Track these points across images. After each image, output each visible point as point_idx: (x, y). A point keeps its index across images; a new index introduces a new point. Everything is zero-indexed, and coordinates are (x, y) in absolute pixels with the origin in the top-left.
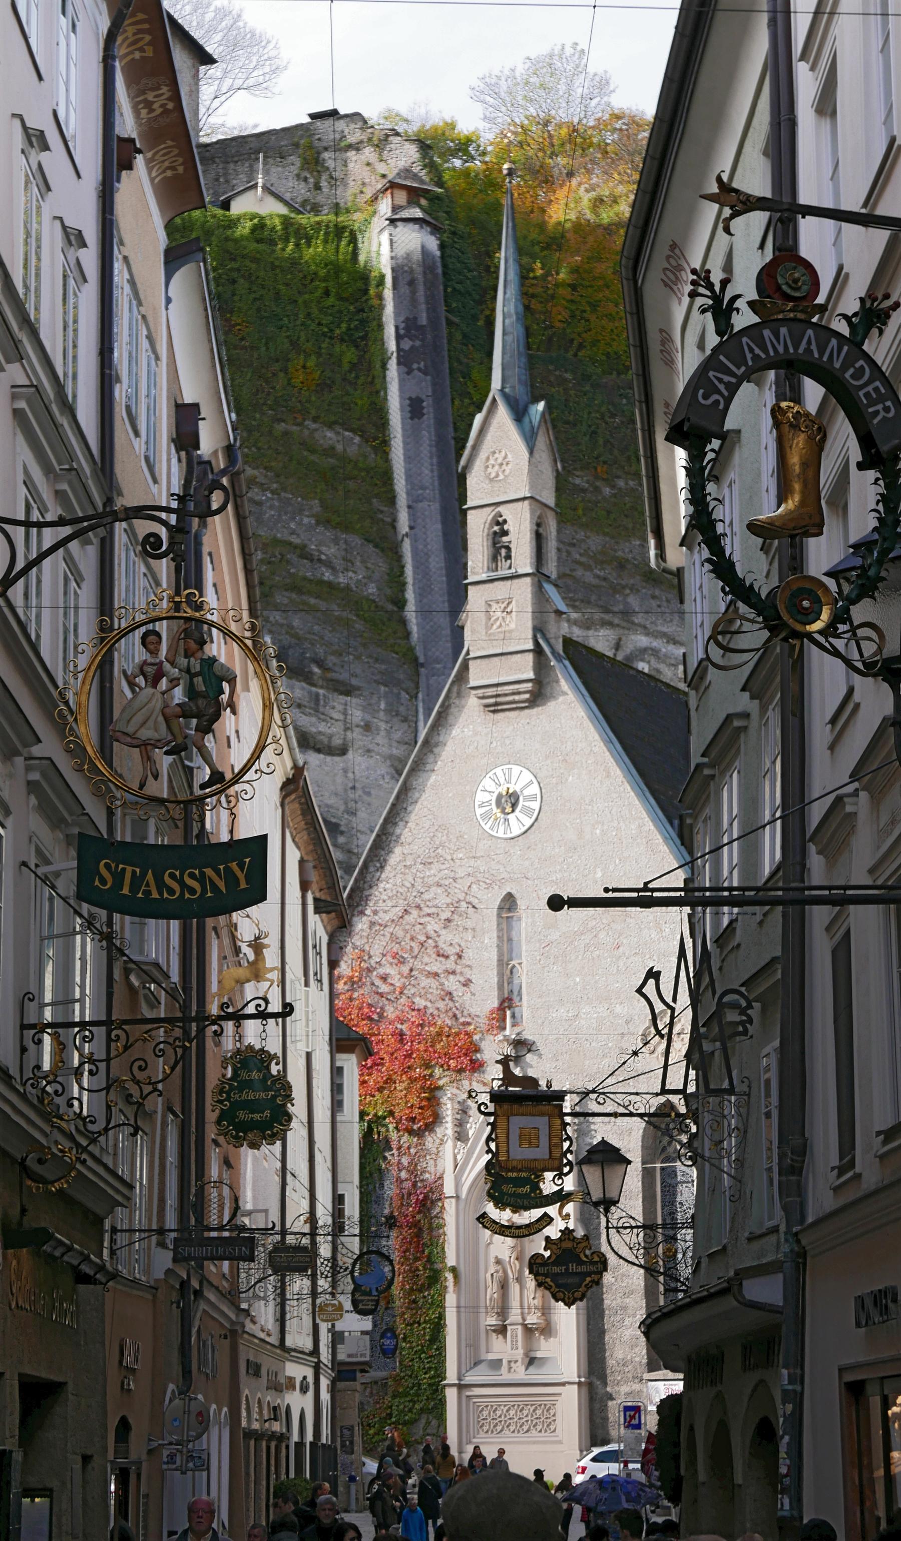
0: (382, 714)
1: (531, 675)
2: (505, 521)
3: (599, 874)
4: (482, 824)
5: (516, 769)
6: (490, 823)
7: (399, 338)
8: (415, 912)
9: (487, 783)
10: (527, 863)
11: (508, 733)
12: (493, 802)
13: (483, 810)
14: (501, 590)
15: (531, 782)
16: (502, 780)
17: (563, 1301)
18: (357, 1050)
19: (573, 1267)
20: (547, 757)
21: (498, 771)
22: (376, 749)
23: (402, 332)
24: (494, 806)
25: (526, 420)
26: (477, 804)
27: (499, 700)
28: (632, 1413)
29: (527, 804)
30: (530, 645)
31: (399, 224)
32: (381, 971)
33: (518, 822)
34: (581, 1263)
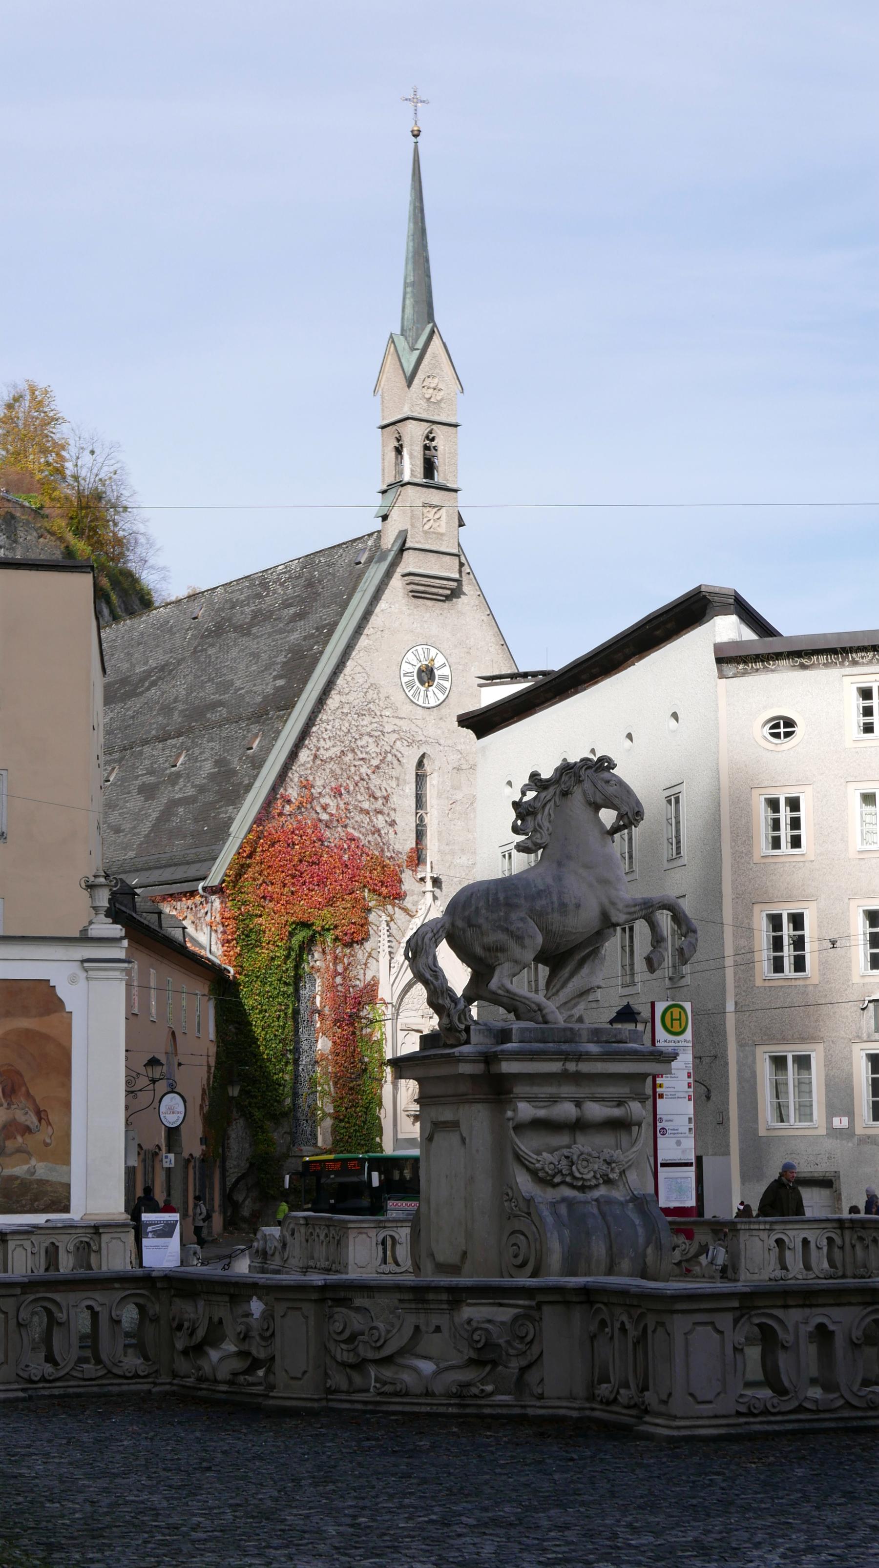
4: (407, 691)
6: (412, 691)
8: (350, 756)
9: (410, 657)
10: (439, 732)
11: (425, 619)
12: (415, 674)
15: (444, 665)
16: (422, 658)
20: (456, 646)
24: (415, 677)
26: (402, 673)
29: (441, 682)
32: (323, 801)
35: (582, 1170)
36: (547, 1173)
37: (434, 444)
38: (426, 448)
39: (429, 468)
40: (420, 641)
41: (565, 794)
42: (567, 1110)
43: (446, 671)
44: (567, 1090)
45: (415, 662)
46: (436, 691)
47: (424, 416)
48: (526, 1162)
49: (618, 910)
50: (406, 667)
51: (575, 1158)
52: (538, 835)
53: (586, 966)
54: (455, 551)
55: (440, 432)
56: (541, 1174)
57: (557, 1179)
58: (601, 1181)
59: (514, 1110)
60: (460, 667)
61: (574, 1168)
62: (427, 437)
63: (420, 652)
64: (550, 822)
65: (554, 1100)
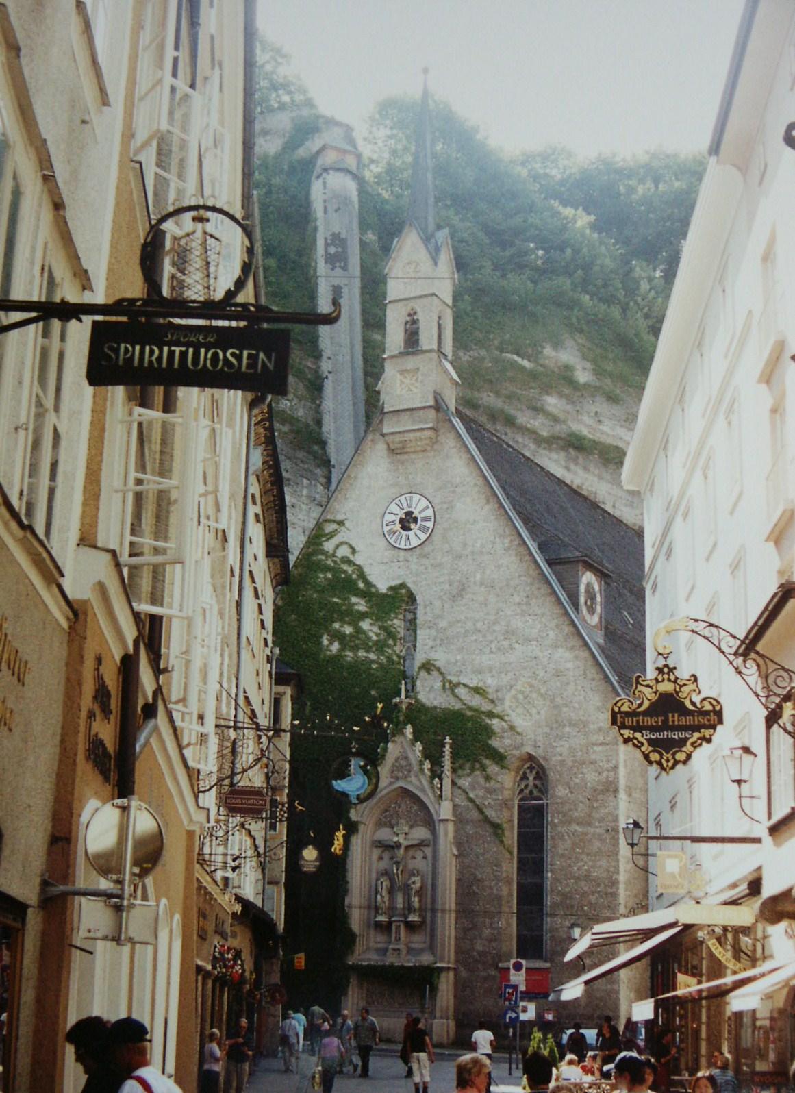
0: (304, 498)
1: (430, 425)
2: (415, 313)
3: (478, 577)
5: (416, 497)
7: (327, 245)
12: (397, 522)
13: (389, 528)
14: (411, 362)
15: (427, 507)
17: (659, 763)
18: (293, 682)
19: (674, 718)
21: (402, 498)
22: (299, 522)
23: (329, 242)
25: (433, 241)
28: (511, 990)
29: (424, 523)
30: (431, 403)
31: (331, 172)
33: (415, 536)
34: (684, 711)
40: (405, 491)
46: (419, 533)
50: (389, 518)
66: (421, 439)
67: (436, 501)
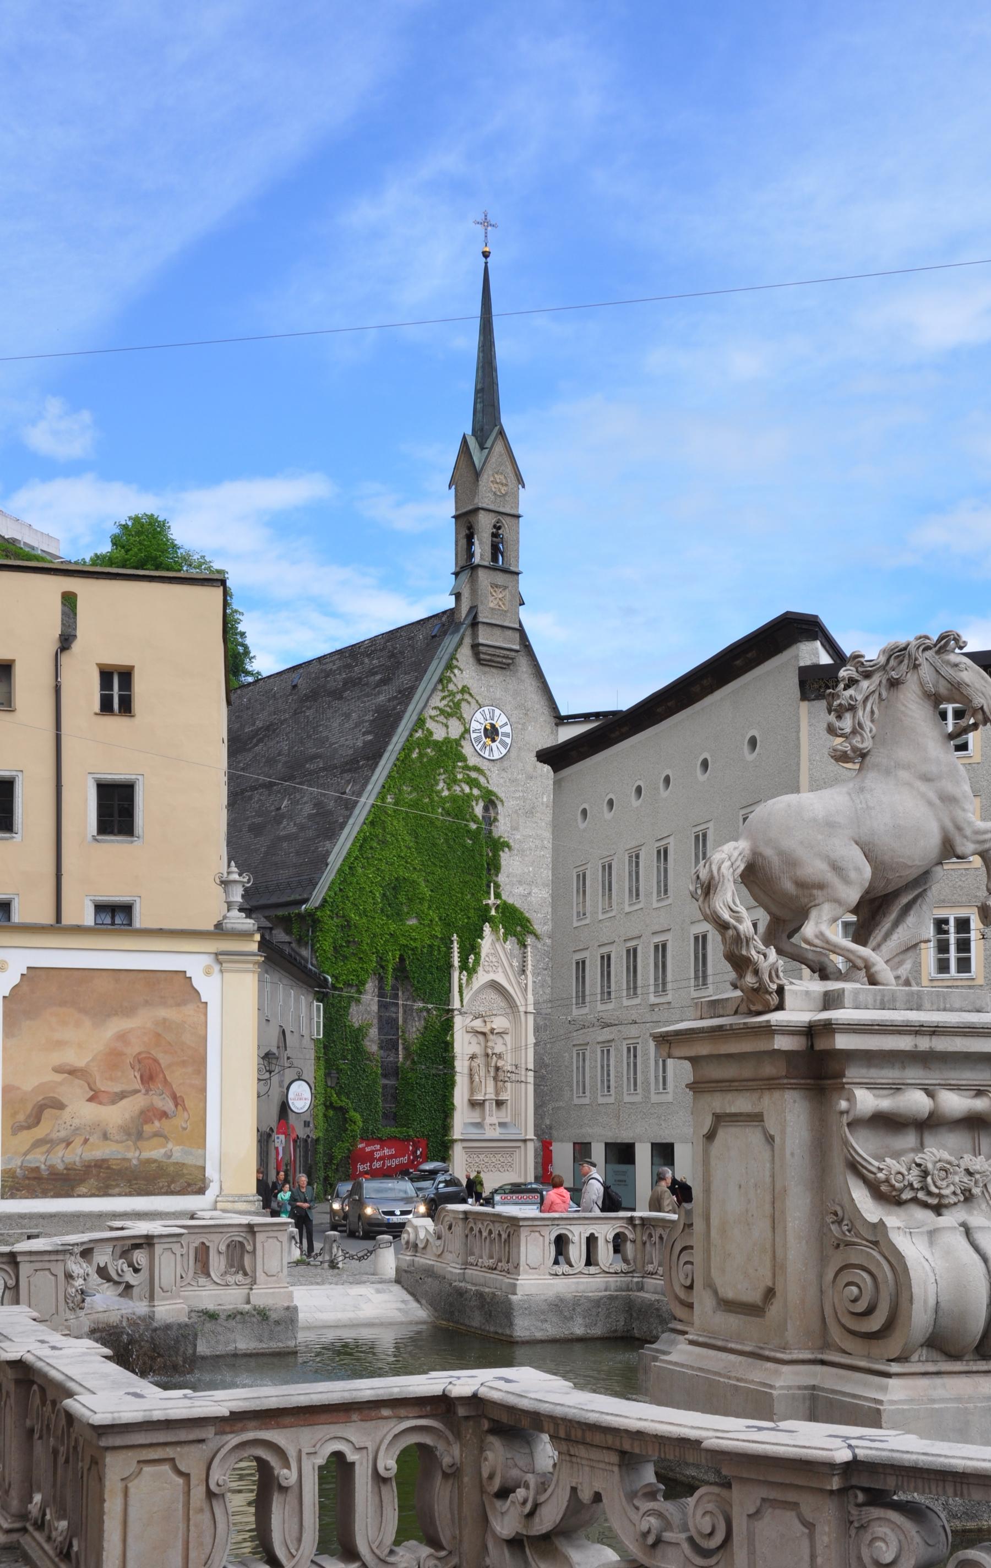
5: (497, 712)
10: (502, 781)
15: (506, 724)
27: (493, 658)
35: (939, 1183)
36: (893, 1186)
37: (500, 532)
38: (494, 535)
39: (496, 551)
41: (894, 684)
42: (916, 1101)
43: (507, 729)
44: (913, 1074)
45: (482, 721)
46: (500, 746)
47: (491, 507)
48: (865, 1171)
49: (966, 837)
51: (930, 1166)
52: (858, 738)
53: (912, 912)
54: (517, 626)
55: (506, 521)
56: (884, 1188)
57: (907, 1195)
58: (962, 1198)
59: (848, 1100)
60: (520, 726)
61: (929, 1179)
62: (495, 526)
63: (487, 712)
64: (872, 721)
65: (897, 1088)
66: (507, 658)
67: (513, 720)
